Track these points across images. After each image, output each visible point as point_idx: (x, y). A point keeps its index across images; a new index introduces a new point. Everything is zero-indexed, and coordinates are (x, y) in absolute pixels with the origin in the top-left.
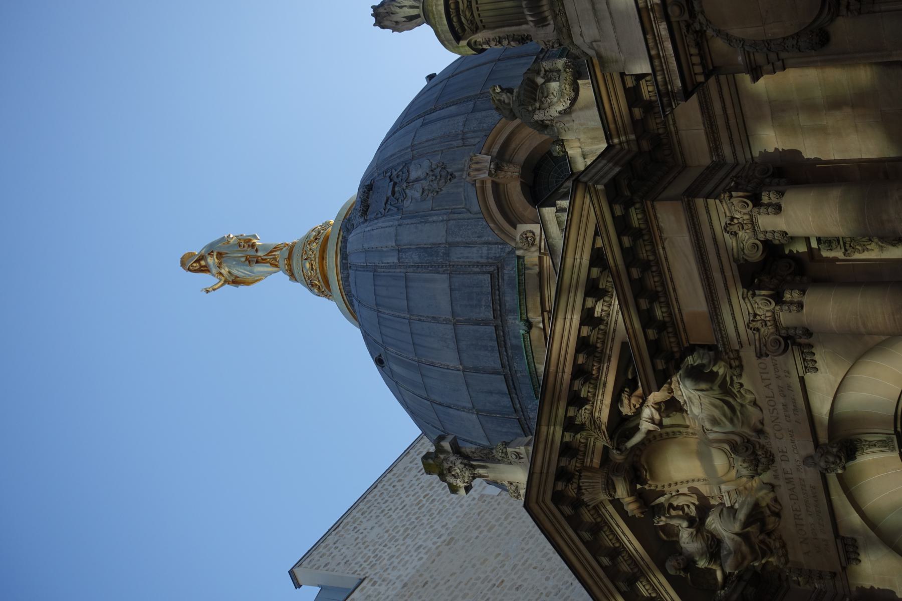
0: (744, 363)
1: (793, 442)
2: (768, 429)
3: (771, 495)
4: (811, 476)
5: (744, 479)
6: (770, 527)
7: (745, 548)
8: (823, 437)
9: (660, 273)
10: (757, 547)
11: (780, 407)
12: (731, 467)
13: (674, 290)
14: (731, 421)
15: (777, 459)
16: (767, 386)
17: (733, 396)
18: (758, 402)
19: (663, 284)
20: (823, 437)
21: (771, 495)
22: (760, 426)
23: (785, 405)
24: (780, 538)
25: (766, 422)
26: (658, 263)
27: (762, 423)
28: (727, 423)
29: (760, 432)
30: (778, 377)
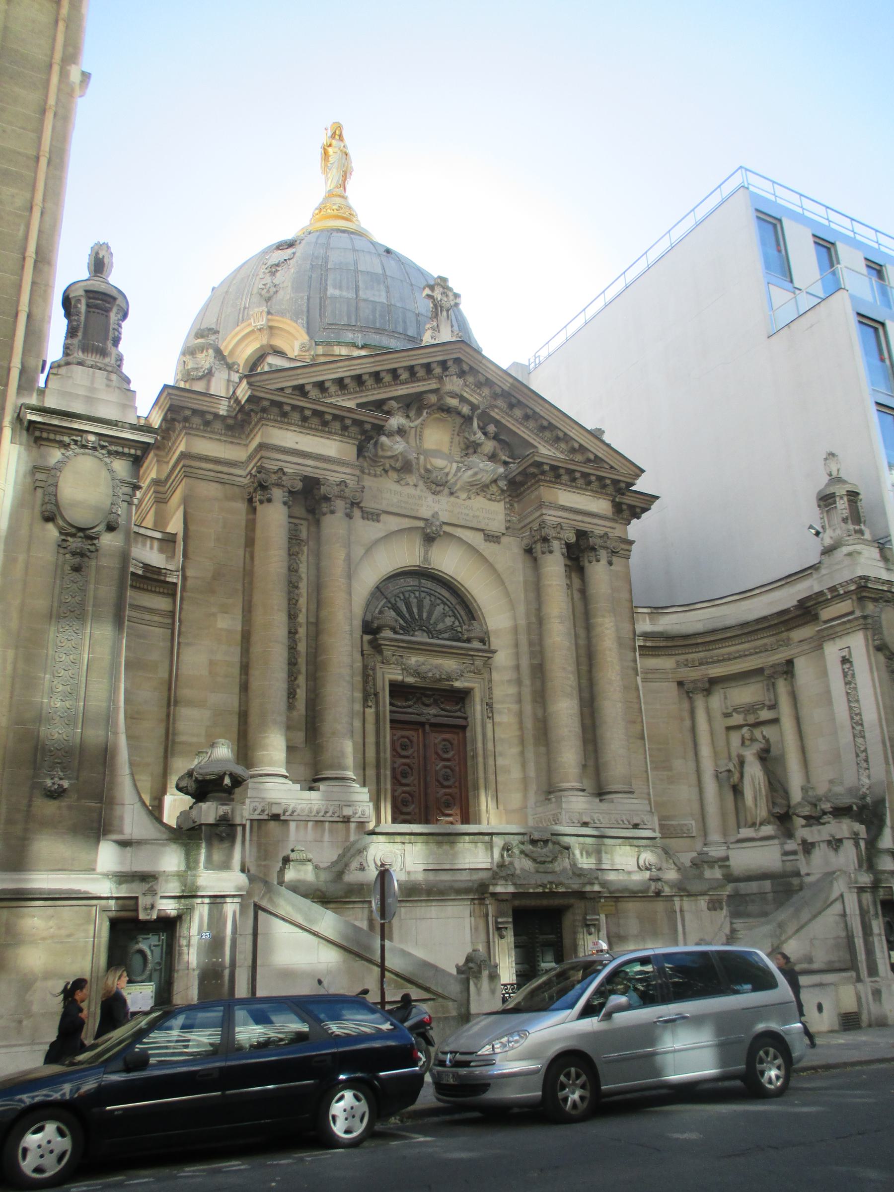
0: (490, 502)
1: (446, 510)
2: (452, 499)
3: (411, 483)
4: (425, 513)
5: (422, 471)
6: (390, 473)
7: (389, 454)
8: (447, 529)
9: (581, 488)
10: (382, 460)
11: (467, 512)
12: (435, 468)
13: (569, 491)
14: (469, 482)
15: (434, 497)
16: (478, 509)
17: (477, 489)
18: (468, 500)
19: (577, 487)
20: (447, 529)
21: (411, 483)
22: (456, 495)
23: (468, 515)
24: (381, 476)
25: (457, 500)
26: (586, 490)
27: (457, 497)
28: (471, 480)
29: (452, 494)
30: (484, 518)
